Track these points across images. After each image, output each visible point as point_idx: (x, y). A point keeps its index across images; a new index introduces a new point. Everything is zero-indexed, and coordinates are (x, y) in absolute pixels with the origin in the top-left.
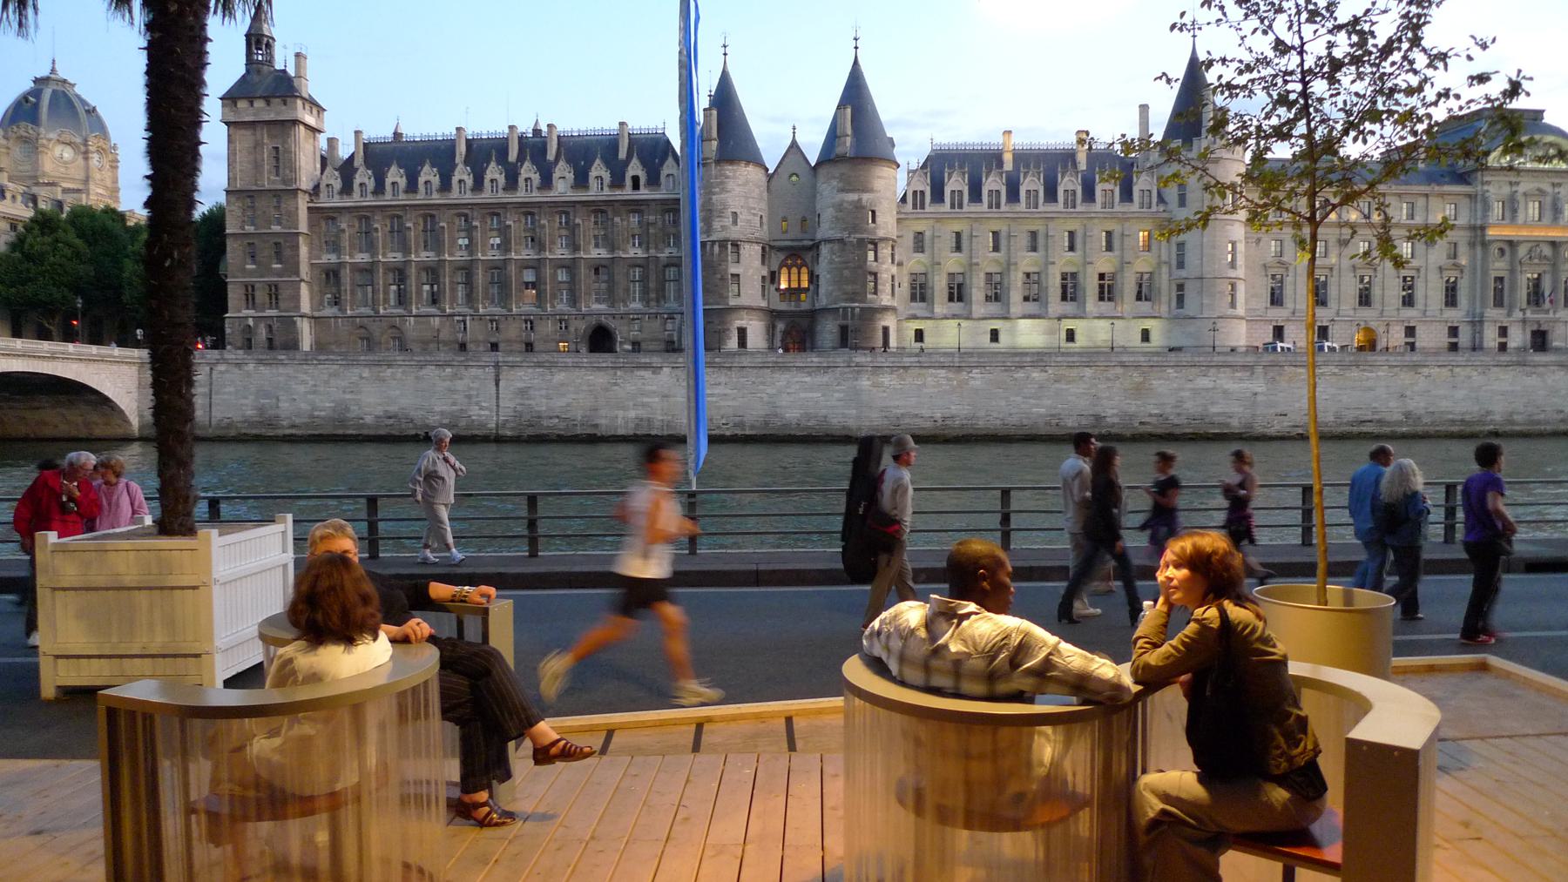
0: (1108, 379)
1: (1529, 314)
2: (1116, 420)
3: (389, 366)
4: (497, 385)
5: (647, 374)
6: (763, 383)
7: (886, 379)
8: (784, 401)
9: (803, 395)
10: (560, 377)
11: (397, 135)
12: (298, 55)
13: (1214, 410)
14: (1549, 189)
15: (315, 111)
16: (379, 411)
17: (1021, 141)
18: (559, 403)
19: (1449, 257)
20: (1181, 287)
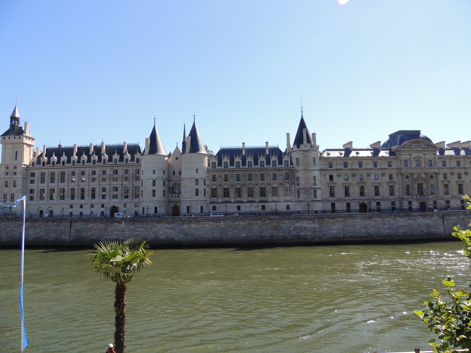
0: (266, 224)
1: (418, 197)
2: (269, 238)
3: (38, 222)
4: (70, 228)
5: (117, 224)
6: (153, 227)
7: (193, 225)
8: (160, 233)
9: (166, 231)
10: (90, 225)
11: (60, 146)
12: (26, 123)
13: (302, 234)
14: (422, 156)
15: (31, 140)
16: (33, 237)
17: (248, 145)
18: (89, 234)
19: (390, 179)
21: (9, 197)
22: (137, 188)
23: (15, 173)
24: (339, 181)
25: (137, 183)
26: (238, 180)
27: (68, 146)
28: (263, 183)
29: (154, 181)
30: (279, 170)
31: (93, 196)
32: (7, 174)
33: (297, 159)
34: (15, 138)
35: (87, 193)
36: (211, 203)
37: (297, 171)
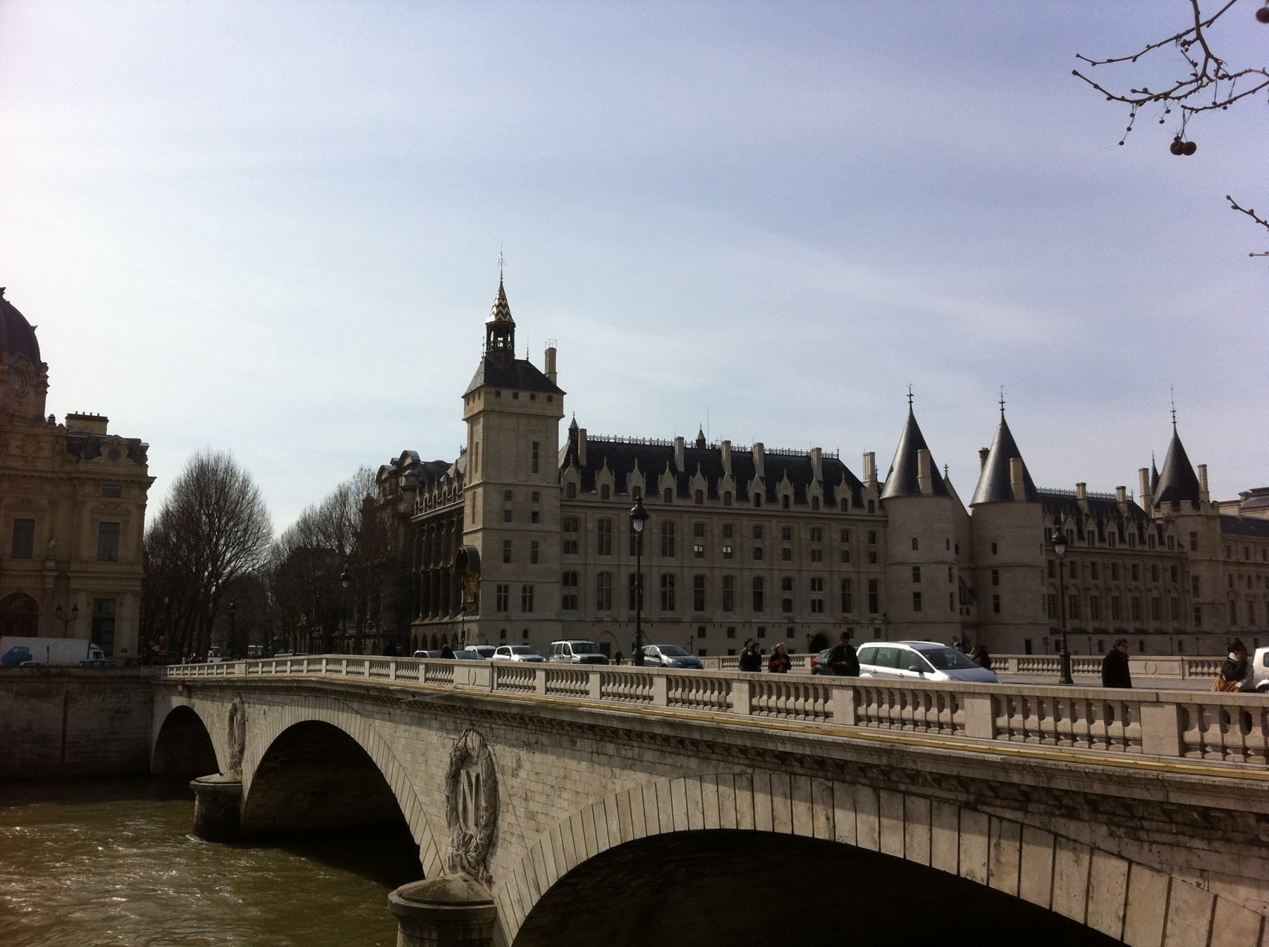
12: (551, 354)
21: (515, 597)
22: (873, 585)
23: (535, 516)
24: (1241, 587)
25: (874, 571)
26: (1095, 577)
27: (640, 438)
28: (1136, 587)
29: (950, 569)
30: (1162, 557)
31: (758, 605)
32: (508, 516)
33: (1193, 534)
34: (533, 398)
35: (744, 590)
36: (1054, 631)
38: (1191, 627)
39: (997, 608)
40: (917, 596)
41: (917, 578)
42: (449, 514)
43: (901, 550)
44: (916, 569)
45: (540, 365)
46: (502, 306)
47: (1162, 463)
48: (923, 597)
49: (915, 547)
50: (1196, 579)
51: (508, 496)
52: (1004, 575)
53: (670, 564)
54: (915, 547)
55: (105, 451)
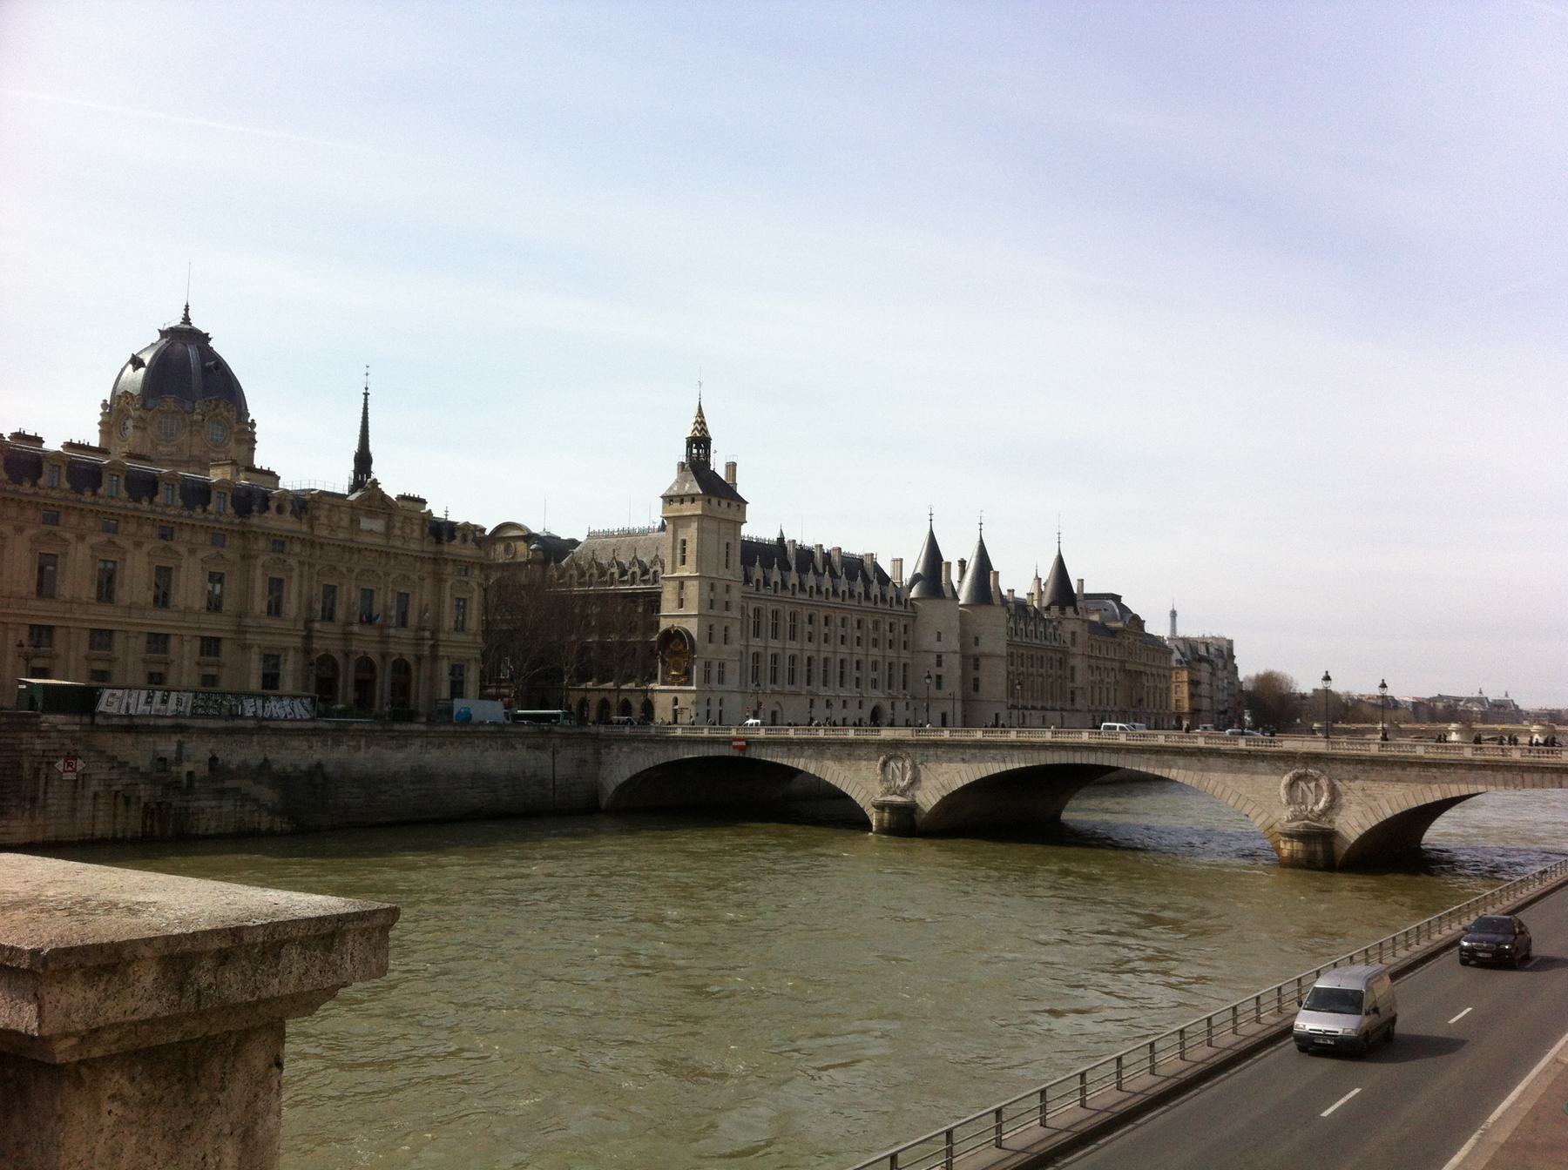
20: (1072, 693)
23: (727, 606)
25: (906, 656)
30: (1055, 650)
32: (712, 605)
33: (1073, 633)
37: (1074, 655)
38: (1068, 706)
39: (976, 688)
40: (939, 677)
41: (939, 664)
42: (634, 597)
43: (928, 640)
44: (939, 657)
45: (723, 476)
46: (701, 422)
47: (1047, 572)
48: (944, 680)
49: (939, 639)
50: (1073, 668)
51: (712, 587)
52: (983, 662)
53: (793, 647)
54: (939, 639)
55: (459, 535)
